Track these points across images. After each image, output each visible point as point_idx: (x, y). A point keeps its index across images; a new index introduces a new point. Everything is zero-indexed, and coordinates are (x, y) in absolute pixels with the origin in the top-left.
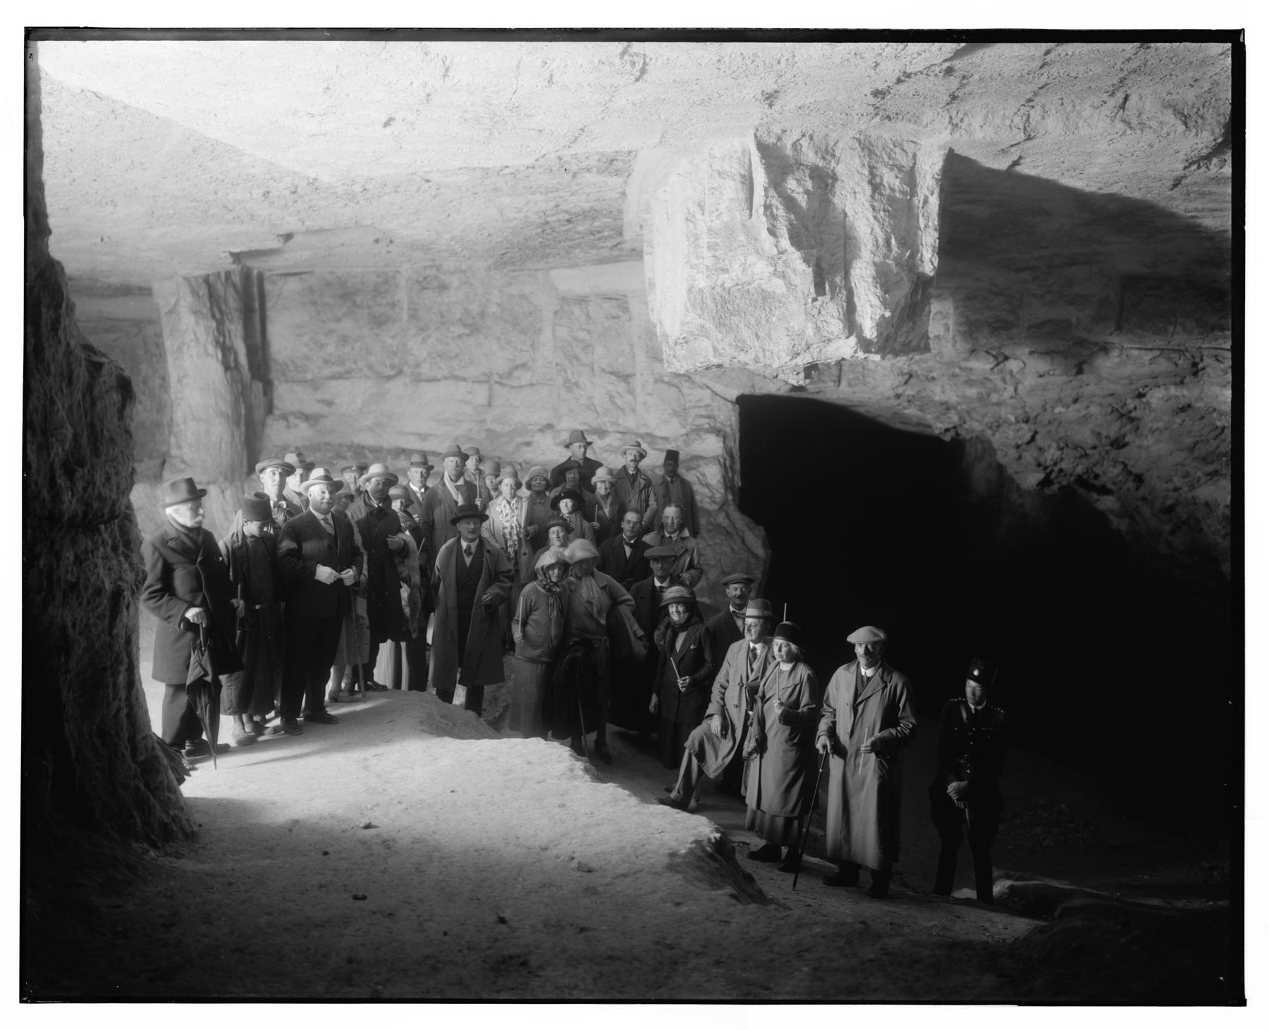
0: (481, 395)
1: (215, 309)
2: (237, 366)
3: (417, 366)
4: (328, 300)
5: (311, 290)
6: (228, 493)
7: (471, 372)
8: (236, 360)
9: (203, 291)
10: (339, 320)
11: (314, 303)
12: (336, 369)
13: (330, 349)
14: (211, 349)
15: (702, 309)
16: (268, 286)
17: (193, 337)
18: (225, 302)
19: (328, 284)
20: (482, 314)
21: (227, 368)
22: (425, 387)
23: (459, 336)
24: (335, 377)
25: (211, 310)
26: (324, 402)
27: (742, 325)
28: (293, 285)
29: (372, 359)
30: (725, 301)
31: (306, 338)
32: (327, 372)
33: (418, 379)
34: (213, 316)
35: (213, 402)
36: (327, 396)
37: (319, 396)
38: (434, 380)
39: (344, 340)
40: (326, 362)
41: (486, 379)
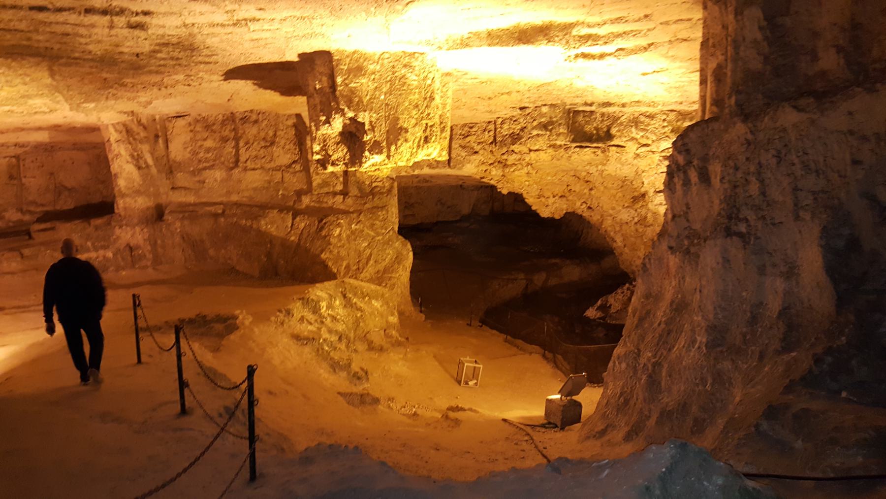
0: (278, 176)
2: (148, 166)
3: (246, 162)
4: (198, 128)
5: (190, 124)
6: (145, 230)
7: (272, 165)
8: (146, 162)
10: (205, 140)
11: (191, 131)
12: (205, 164)
13: (201, 155)
14: (130, 160)
16: (170, 125)
18: (138, 134)
19: (197, 121)
20: (275, 135)
21: (139, 168)
22: (250, 173)
23: (265, 147)
24: (205, 169)
25: (128, 139)
26: (199, 182)
28: (181, 122)
29: (223, 159)
31: (189, 150)
32: (201, 166)
33: (245, 169)
34: (130, 143)
36: (202, 178)
37: (197, 179)
38: (254, 169)
39: (208, 150)
40: (200, 161)
41: (278, 169)
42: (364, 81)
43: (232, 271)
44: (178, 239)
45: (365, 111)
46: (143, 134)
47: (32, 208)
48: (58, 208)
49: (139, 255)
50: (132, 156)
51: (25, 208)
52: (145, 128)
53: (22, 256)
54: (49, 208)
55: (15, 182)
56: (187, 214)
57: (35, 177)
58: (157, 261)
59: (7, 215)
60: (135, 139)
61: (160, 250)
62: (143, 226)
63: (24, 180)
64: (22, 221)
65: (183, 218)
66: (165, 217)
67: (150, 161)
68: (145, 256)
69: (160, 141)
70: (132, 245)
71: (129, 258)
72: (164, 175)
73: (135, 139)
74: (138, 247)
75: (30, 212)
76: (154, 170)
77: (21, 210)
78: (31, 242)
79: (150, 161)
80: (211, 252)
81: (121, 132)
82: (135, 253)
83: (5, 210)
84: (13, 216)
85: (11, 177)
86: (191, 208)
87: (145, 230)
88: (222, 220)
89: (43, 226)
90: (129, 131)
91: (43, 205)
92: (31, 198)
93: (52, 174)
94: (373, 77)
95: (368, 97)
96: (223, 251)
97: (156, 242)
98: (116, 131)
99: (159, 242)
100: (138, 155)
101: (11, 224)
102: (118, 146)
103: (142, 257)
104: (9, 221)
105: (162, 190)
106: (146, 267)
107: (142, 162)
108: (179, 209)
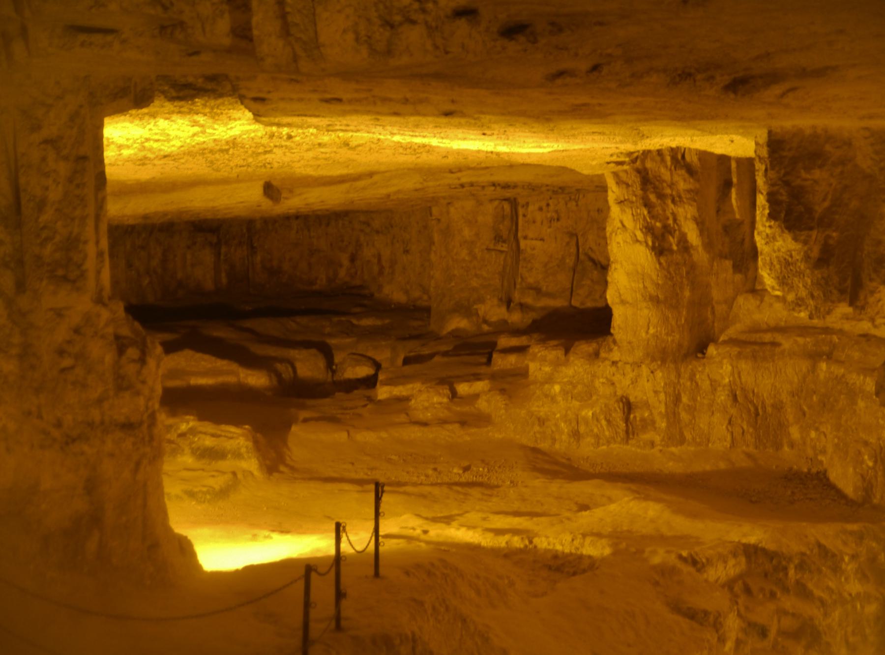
1: (652, 197)
2: (685, 246)
6: (659, 374)
8: (683, 241)
9: (635, 180)
14: (640, 235)
15: (771, 269)
17: (619, 225)
18: (672, 185)
21: (660, 250)
27: (801, 285)
30: (788, 264)
34: (647, 204)
35: (641, 286)
42: (817, 174)
43: (822, 480)
44: (722, 397)
45: (811, 229)
46: (683, 183)
47: (529, 300)
48: (576, 303)
49: (643, 420)
50: (648, 229)
51: (517, 296)
52: (690, 171)
53: (454, 394)
54: (558, 303)
55: (505, 247)
56: (748, 350)
57: (542, 240)
58: (676, 436)
59: (482, 309)
60: (661, 196)
61: (684, 416)
62: (654, 366)
63: (523, 244)
64: (505, 322)
65: (739, 355)
66: (712, 350)
67: (693, 236)
68: (653, 422)
69: (734, 192)
70: (632, 399)
71: (623, 425)
72: (728, 264)
73: (661, 196)
74: (647, 405)
75: (523, 307)
76: (701, 256)
77: (508, 302)
78: (483, 370)
79: (693, 236)
80: (795, 432)
81: (628, 185)
82: (637, 415)
83: (481, 300)
84: (493, 311)
85: (498, 238)
86: (768, 337)
87: (659, 374)
88: (823, 366)
89: (514, 342)
90: (646, 179)
91: (549, 295)
92: (531, 280)
93: (573, 235)
94: (839, 170)
95: (826, 204)
96: (813, 434)
97: (677, 399)
98: (619, 182)
99: (685, 399)
100: (665, 227)
101: (486, 328)
102: (623, 211)
103: (648, 424)
104: (485, 321)
105: (716, 294)
106: (652, 444)
107: (673, 241)
108: (743, 337)
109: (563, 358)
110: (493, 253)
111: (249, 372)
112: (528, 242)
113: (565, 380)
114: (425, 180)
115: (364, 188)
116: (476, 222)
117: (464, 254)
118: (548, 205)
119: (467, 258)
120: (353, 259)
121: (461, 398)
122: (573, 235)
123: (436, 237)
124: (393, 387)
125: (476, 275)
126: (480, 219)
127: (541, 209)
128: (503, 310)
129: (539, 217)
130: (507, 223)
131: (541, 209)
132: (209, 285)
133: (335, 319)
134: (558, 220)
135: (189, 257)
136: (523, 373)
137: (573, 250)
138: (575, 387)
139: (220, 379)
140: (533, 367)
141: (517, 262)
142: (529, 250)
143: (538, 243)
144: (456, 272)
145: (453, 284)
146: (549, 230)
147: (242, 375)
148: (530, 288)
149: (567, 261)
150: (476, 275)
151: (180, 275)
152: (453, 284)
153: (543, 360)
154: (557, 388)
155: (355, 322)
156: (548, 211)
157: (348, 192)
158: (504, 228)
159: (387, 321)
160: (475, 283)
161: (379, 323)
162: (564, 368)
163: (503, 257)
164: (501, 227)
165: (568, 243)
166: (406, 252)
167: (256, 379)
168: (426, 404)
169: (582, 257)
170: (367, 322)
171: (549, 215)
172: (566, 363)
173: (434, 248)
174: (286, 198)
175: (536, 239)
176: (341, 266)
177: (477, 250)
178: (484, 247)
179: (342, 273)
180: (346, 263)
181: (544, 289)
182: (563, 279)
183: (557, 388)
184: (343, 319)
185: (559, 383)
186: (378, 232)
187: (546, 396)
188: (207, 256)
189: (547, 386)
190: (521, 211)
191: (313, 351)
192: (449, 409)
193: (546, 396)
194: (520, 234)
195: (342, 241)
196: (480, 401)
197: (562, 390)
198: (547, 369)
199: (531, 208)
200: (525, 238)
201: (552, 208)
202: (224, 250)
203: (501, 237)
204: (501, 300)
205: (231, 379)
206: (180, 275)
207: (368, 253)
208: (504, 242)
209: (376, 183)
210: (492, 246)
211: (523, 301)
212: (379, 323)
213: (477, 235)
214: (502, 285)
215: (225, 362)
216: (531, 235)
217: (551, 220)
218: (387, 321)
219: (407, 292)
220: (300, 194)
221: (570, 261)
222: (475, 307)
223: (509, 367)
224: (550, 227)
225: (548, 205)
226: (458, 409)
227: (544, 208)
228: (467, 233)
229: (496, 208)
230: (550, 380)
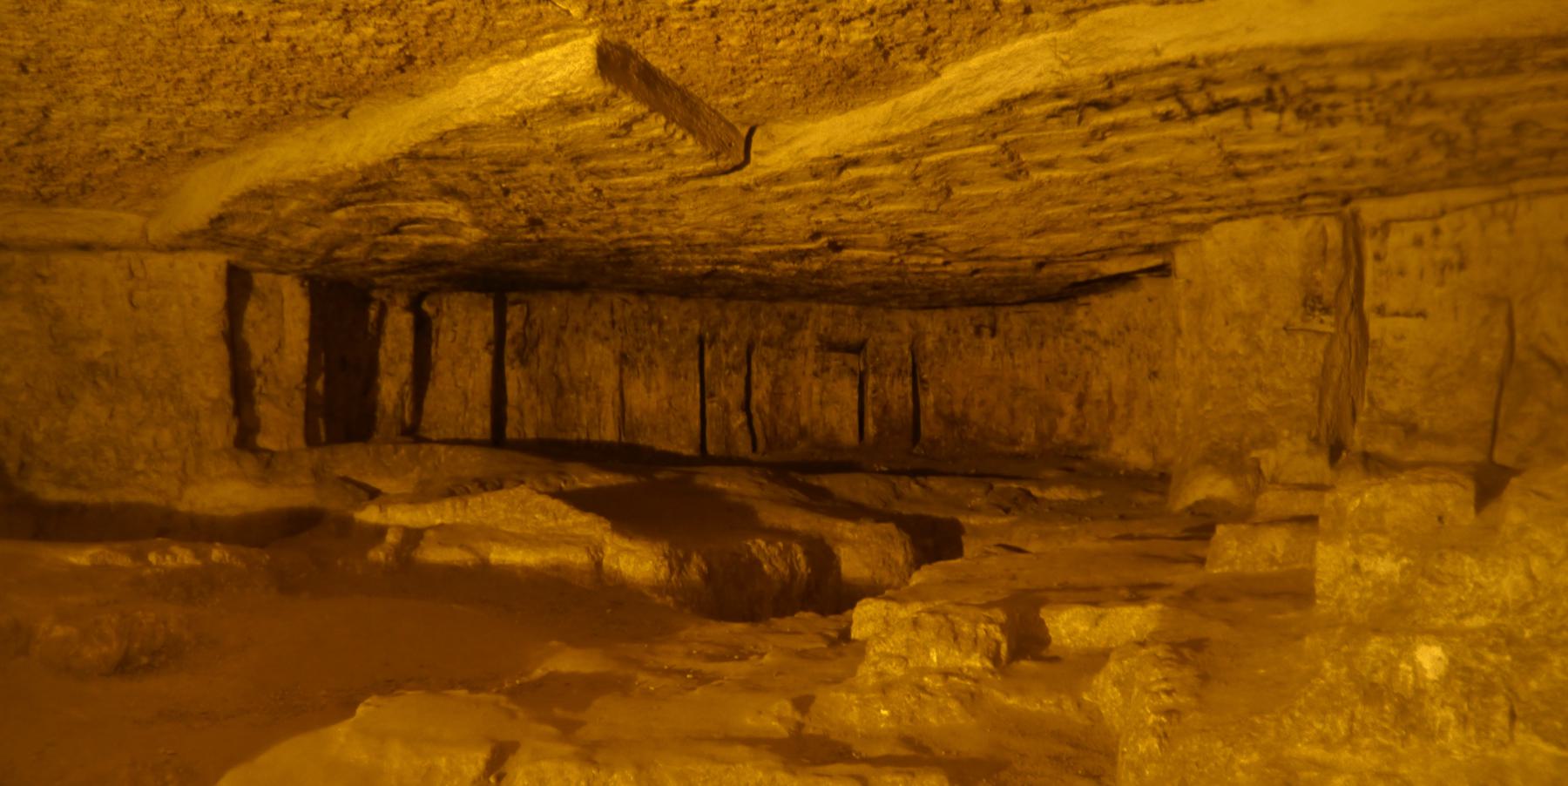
51: (1357, 439)
55: (1327, 324)
57: (1422, 314)
59: (1269, 459)
63: (1375, 326)
83: (1269, 440)
85: (1312, 303)
92: (1393, 406)
93: (1494, 300)
109: (1467, 517)
110: (1300, 337)
111: (627, 544)
112: (1391, 323)
113: (1478, 621)
114: (1065, 64)
115: (923, 107)
116: (1263, 270)
117: (1234, 341)
118: (1436, 232)
119: (1241, 351)
120: (1080, 402)
121: (1055, 659)
122: (1497, 299)
123: (1184, 317)
124: (894, 606)
125: (1260, 387)
126: (1271, 261)
127: (1418, 242)
128: (1321, 462)
129: (1413, 259)
130: (1334, 266)
131: (1418, 242)
132: (849, 436)
133: (999, 485)
134: (1462, 266)
135: (816, 389)
136: (1296, 590)
137: (1500, 333)
138: (1529, 660)
139: (552, 556)
140: (1328, 559)
141: (1362, 363)
142: (1389, 341)
143: (1413, 324)
144: (1215, 380)
145: (1208, 407)
146: (1438, 292)
147: (609, 550)
148: (1390, 419)
149: (1485, 359)
150: (1260, 387)
151: (804, 420)
152: (1208, 407)
153: (1372, 522)
154: (1430, 658)
155: (1035, 492)
156: (1437, 247)
157: (888, 123)
158: (1327, 278)
159: (1097, 494)
160: (1256, 403)
161: (1080, 496)
162: (1469, 565)
163: (1321, 345)
164: (1318, 274)
165: (1486, 320)
166: (1154, 375)
167: (636, 562)
168: (895, 670)
169: (1522, 354)
170: (1057, 494)
171: (1439, 256)
172: (1481, 544)
173: (1181, 343)
174: (761, 154)
175: (1407, 315)
176: (1062, 414)
177: (1262, 333)
178: (1279, 324)
179: (1064, 426)
180: (1070, 409)
181: (1425, 424)
182: (1473, 401)
183: (1430, 658)
184: (1014, 485)
185: (1440, 635)
186: (1106, 343)
187: (1372, 693)
188: (846, 391)
189: (1375, 644)
190: (1370, 246)
191: (889, 527)
192: (971, 699)
193: (1372, 693)
194: (1368, 303)
195: (1065, 373)
196: (1100, 680)
197: (1456, 670)
198: (1385, 567)
199: (1394, 239)
200: (1381, 311)
201: (1446, 237)
202: (871, 381)
203: (1319, 298)
204: (1315, 440)
205: (578, 558)
206: (804, 420)
207: (1098, 387)
208: (1326, 310)
209: (949, 89)
210: (1297, 322)
211: (1369, 448)
212: (1080, 496)
213: (1263, 298)
214: (1320, 408)
215: (585, 518)
216: (1394, 303)
217: (1445, 266)
218: (1097, 494)
219: (1153, 450)
220: (788, 142)
221: (1491, 360)
222: (1254, 454)
223: (1263, 568)
224: (1441, 284)
225: (1436, 232)
226: (1012, 701)
227: (1428, 239)
228: (1242, 296)
229: (1309, 234)
230: (1397, 617)
